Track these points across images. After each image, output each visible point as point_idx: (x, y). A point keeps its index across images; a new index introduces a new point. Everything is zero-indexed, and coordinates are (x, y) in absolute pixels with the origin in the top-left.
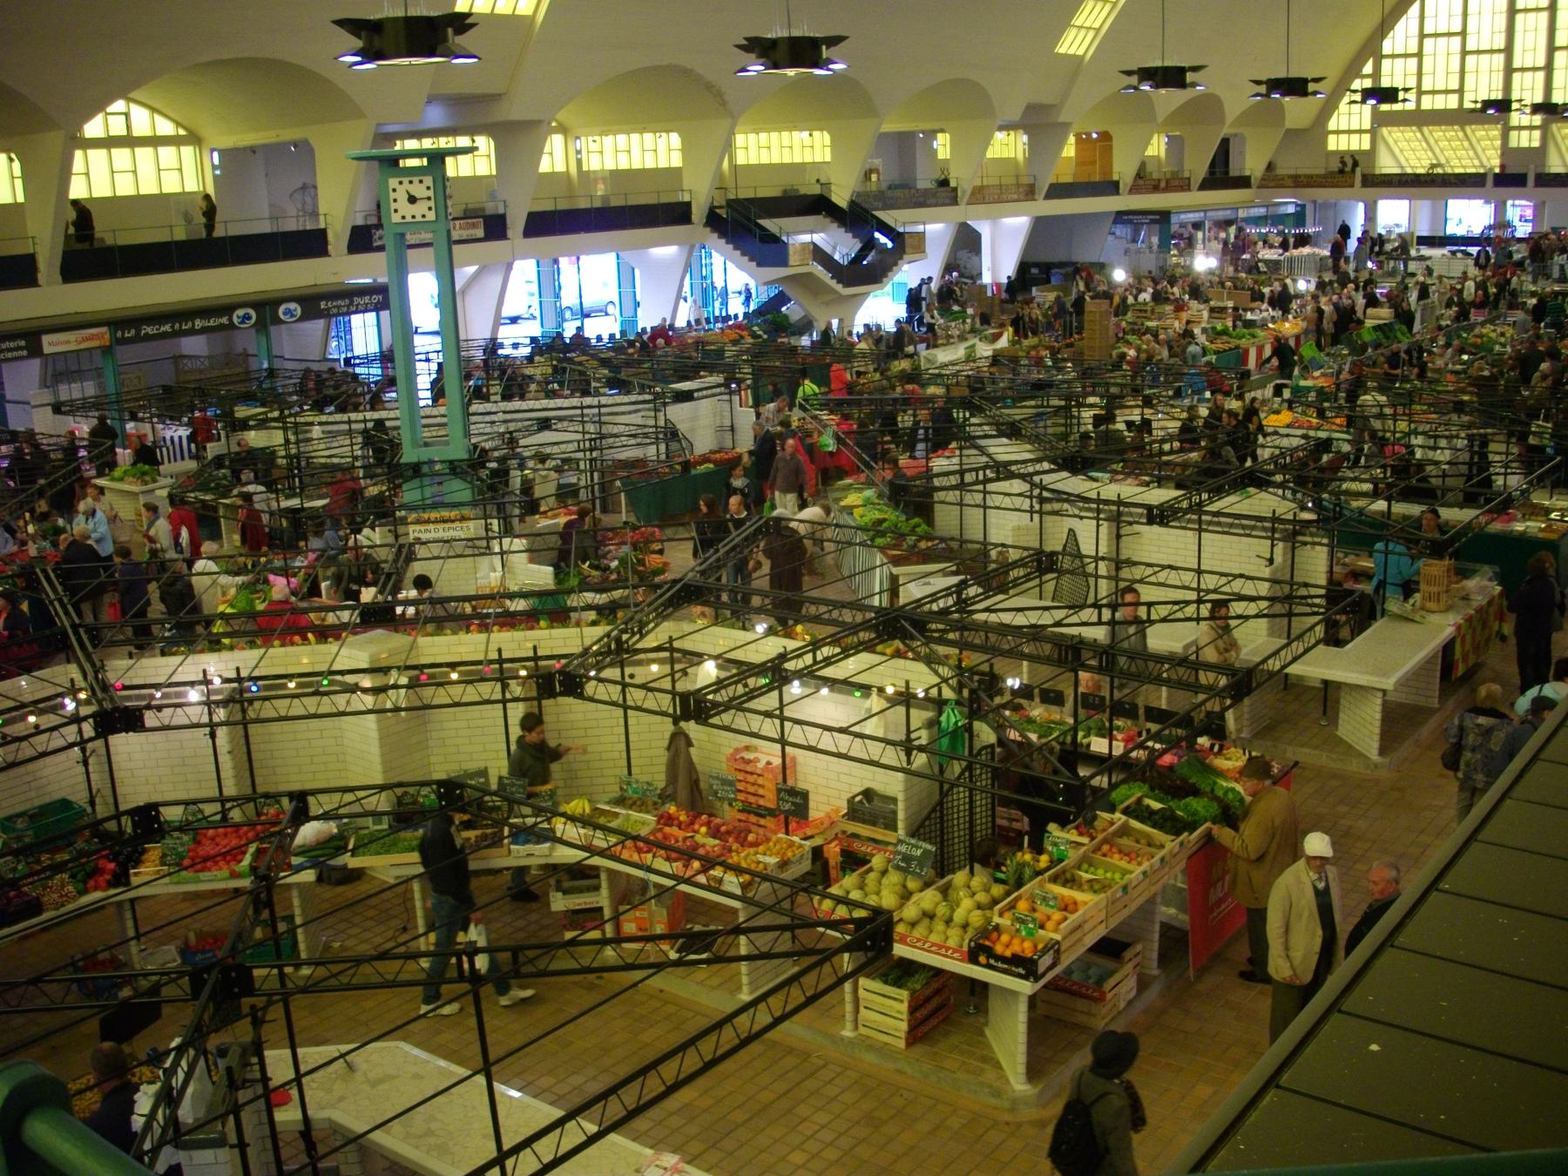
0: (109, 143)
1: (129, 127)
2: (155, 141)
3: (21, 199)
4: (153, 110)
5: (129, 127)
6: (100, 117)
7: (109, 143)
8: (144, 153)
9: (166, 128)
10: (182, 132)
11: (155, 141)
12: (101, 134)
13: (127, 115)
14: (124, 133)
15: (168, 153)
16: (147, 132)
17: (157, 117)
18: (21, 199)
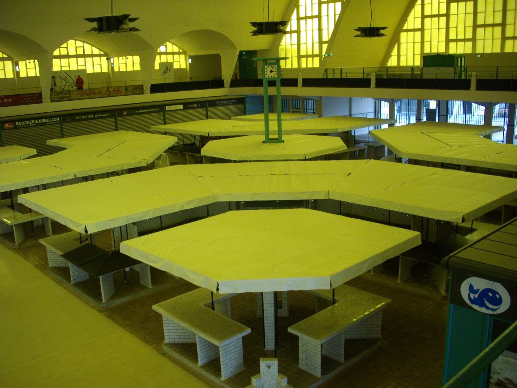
0: (60, 57)
1: (68, 52)
2: (92, 56)
3: (38, 75)
4: (92, 45)
5: (68, 52)
6: (58, 50)
7: (60, 57)
8: (89, 60)
9: (96, 51)
10: (102, 53)
11: (92, 56)
12: (58, 54)
13: (83, 47)
14: (66, 54)
15: (97, 60)
16: (90, 53)
17: (93, 47)
18: (38, 75)
